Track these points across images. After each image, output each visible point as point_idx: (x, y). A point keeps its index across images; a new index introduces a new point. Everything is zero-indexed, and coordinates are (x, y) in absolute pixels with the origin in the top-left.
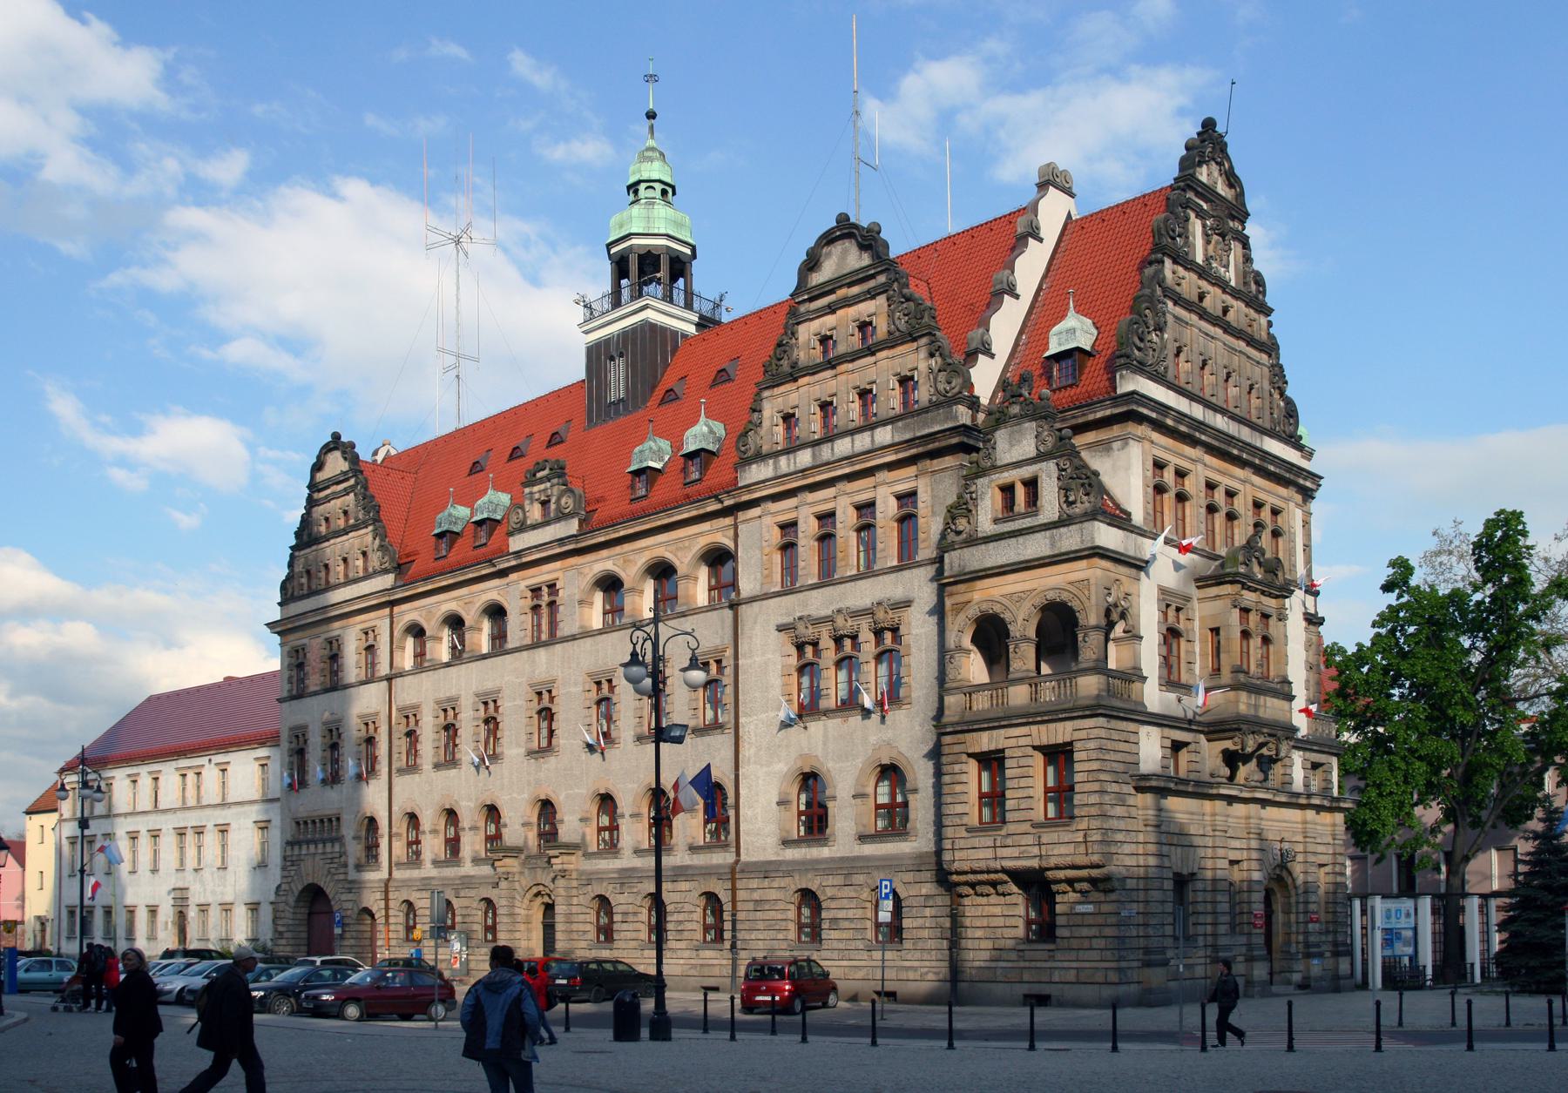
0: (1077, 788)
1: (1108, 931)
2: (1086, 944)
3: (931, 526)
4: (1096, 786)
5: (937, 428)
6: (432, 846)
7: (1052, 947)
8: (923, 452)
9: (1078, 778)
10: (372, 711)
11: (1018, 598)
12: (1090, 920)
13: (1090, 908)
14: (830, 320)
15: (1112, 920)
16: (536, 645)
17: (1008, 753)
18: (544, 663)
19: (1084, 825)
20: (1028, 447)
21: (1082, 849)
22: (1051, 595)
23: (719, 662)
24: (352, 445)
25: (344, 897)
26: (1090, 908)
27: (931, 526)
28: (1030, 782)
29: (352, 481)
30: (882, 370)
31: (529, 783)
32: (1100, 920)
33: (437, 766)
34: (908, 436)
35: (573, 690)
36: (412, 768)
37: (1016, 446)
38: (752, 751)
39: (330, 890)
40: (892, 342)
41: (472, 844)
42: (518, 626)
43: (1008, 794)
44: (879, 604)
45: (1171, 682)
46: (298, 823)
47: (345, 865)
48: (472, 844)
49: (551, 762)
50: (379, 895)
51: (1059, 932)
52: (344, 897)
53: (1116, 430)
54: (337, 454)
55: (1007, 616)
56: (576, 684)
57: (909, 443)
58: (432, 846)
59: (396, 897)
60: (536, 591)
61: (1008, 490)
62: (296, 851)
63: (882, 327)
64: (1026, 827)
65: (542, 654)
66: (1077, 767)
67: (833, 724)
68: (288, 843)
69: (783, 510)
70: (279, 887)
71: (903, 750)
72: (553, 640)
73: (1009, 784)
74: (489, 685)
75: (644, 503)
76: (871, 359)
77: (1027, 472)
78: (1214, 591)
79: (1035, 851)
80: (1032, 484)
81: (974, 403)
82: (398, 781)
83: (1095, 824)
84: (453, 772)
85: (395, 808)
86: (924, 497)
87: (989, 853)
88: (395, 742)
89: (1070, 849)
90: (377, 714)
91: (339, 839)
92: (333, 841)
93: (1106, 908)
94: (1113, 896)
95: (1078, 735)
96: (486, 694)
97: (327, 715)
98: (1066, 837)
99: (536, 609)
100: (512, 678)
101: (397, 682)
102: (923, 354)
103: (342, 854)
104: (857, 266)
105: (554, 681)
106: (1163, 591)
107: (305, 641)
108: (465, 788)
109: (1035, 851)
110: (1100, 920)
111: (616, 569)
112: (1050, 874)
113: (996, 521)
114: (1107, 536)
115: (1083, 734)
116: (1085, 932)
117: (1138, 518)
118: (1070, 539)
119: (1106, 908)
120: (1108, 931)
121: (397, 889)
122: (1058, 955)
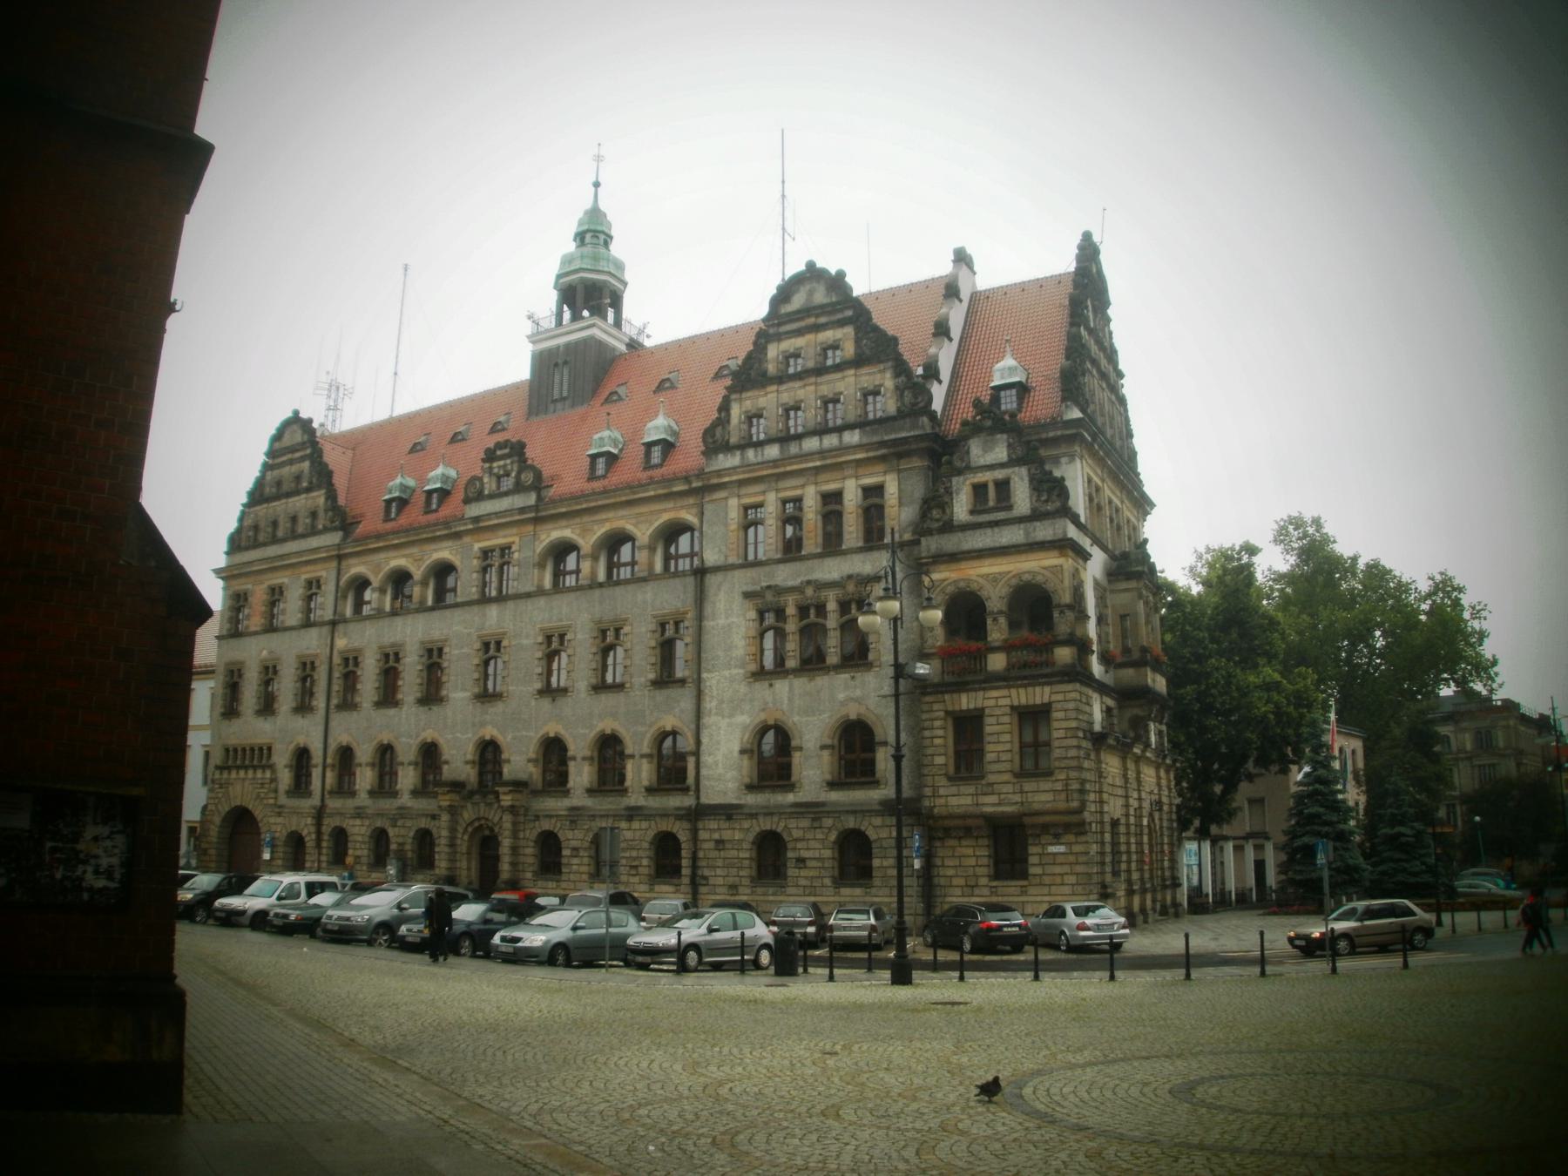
0: (1056, 744)
1: (1079, 869)
2: (1058, 880)
3: (899, 514)
4: (1074, 742)
5: (904, 435)
6: (365, 778)
7: (1025, 883)
8: (894, 454)
9: (1056, 734)
10: (311, 652)
11: (994, 579)
12: (1060, 859)
13: (1062, 849)
14: (800, 342)
15: (1082, 859)
16: (484, 600)
17: (987, 711)
18: (493, 618)
19: (1063, 776)
20: (1000, 453)
21: (1063, 796)
22: (1026, 577)
23: (677, 624)
24: (310, 421)
25: (272, 820)
26: (1062, 849)
27: (899, 514)
28: (1001, 741)
29: (308, 451)
30: (848, 384)
31: (474, 725)
32: (1072, 858)
33: (379, 704)
34: (876, 439)
35: (525, 642)
36: (348, 704)
37: (989, 453)
38: (714, 704)
39: (258, 813)
40: (858, 362)
41: (407, 778)
42: (466, 583)
43: (989, 748)
44: (850, 577)
45: (1106, 659)
46: (227, 750)
47: (276, 791)
48: (407, 778)
49: (498, 708)
50: (309, 820)
51: (1032, 870)
52: (272, 820)
53: (1063, 450)
54: (295, 427)
55: (984, 594)
56: (527, 637)
57: (882, 444)
58: (365, 778)
59: (329, 824)
60: (486, 553)
61: (979, 490)
62: (225, 775)
63: (849, 350)
64: (1006, 777)
65: (493, 611)
66: (1055, 725)
67: (800, 684)
68: (217, 767)
69: (751, 495)
70: (205, 808)
71: (872, 707)
72: (501, 598)
73: (988, 739)
74: (436, 634)
75: (605, 482)
76: (839, 375)
77: (1000, 474)
78: (1124, 585)
79: (1017, 798)
80: (1003, 487)
81: (932, 415)
82: (338, 720)
83: (1073, 774)
84: (392, 712)
85: (330, 741)
86: (892, 488)
87: (969, 801)
88: (335, 681)
89: (1049, 797)
90: (317, 655)
91: (271, 767)
92: (264, 768)
93: (1077, 848)
94: (1083, 839)
95: (1054, 698)
96: (431, 642)
97: (265, 653)
98: (1045, 785)
99: (484, 570)
100: (458, 631)
101: (340, 627)
102: (888, 375)
103: (273, 780)
104: (826, 301)
105: (504, 634)
106: (1096, 583)
107: (249, 586)
108: (407, 726)
109: (1017, 798)
110: (1072, 858)
111: (574, 537)
112: (1027, 820)
113: (972, 512)
114: (1072, 532)
115: (1060, 697)
116: (1058, 870)
117: (1083, 520)
118: (1043, 531)
119: (1077, 848)
120: (1079, 869)
121: (331, 815)
122: (1032, 890)
